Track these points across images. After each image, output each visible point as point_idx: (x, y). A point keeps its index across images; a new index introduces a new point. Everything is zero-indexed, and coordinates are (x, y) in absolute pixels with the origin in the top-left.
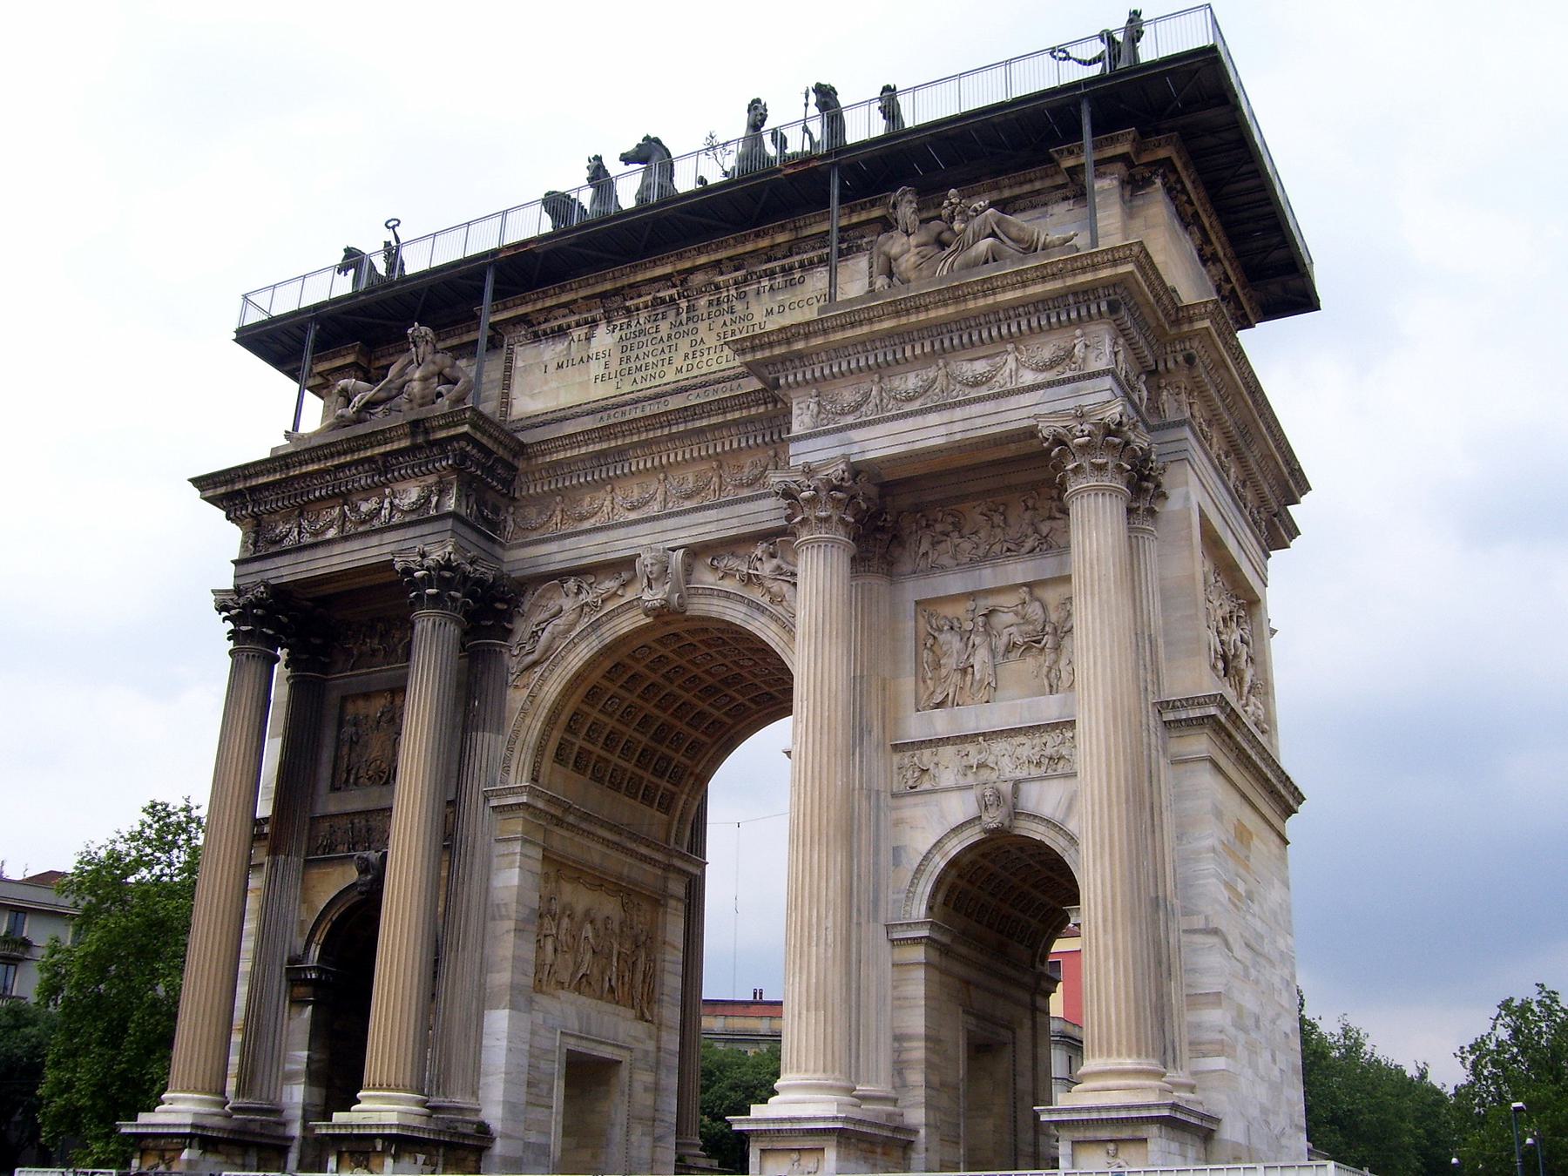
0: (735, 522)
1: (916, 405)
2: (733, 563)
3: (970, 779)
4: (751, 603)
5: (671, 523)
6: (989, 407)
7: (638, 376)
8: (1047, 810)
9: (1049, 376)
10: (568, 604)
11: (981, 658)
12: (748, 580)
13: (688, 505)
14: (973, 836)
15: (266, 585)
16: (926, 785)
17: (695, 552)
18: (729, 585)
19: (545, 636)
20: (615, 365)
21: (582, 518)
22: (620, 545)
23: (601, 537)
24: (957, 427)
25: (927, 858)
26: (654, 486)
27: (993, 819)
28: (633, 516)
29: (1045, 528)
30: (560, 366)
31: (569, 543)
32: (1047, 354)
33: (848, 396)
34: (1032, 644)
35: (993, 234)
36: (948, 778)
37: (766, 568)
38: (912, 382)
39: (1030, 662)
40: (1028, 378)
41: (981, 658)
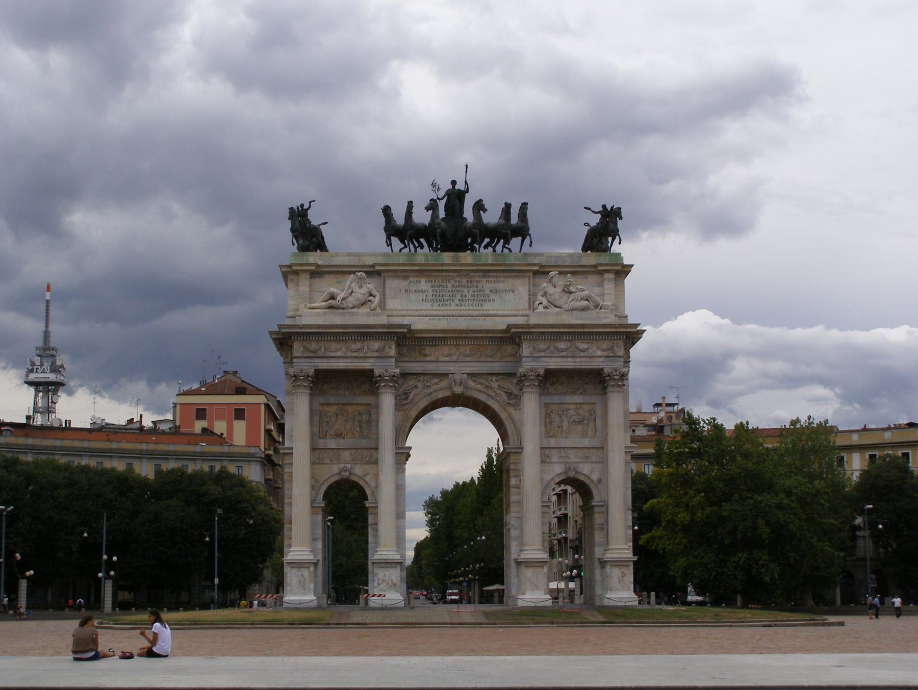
1: (564, 354)
2: (483, 381)
4: (489, 395)
6: (588, 360)
7: (440, 303)
8: (585, 472)
10: (420, 385)
11: (565, 424)
12: (487, 387)
13: (467, 359)
14: (563, 477)
16: (548, 460)
18: (479, 387)
19: (411, 396)
20: (430, 297)
21: (426, 356)
25: (549, 482)
26: (454, 350)
27: (572, 474)
28: (446, 359)
29: (586, 386)
30: (406, 291)
31: (421, 364)
32: (605, 346)
34: (580, 422)
36: (554, 459)
37: (495, 385)
38: (562, 345)
39: (579, 428)
40: (599, 353)
41: (565, 424)
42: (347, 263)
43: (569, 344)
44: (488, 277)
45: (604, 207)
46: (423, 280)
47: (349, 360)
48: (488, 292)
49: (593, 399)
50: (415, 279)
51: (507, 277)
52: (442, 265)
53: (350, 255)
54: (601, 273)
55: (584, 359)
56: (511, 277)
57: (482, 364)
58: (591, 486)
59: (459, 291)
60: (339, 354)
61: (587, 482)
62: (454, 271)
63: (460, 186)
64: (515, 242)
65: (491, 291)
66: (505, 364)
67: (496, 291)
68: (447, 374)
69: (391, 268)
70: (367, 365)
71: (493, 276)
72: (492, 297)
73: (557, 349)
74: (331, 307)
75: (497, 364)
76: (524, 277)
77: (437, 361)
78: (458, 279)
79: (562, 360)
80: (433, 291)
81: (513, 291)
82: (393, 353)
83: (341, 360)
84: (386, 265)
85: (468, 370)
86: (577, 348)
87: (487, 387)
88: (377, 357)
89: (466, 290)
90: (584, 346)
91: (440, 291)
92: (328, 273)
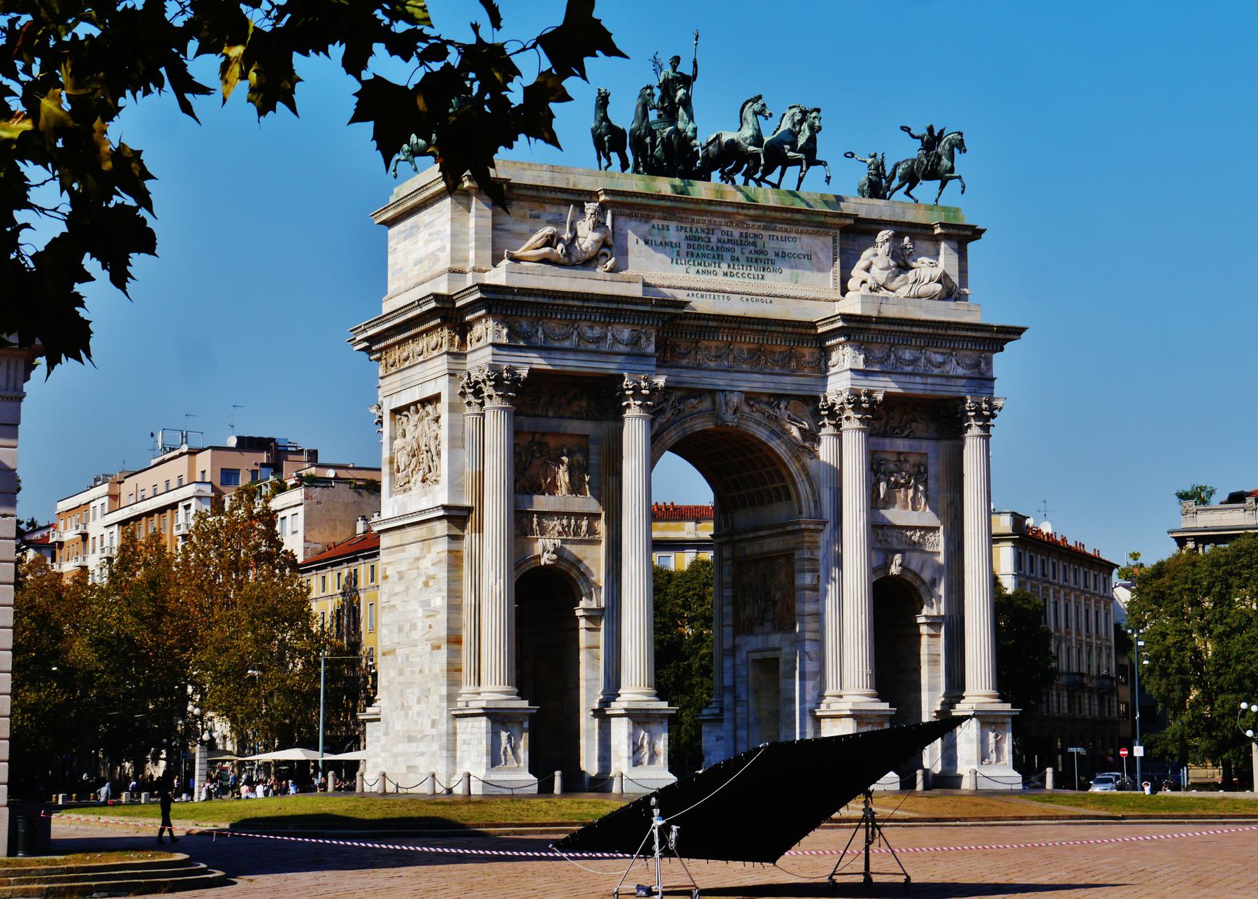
0: (772, 385)
1: (909, 369)
3: (878, 546)
4: (773, 432)
5: (737, 375)
6: (943, 381)
9: (968, 372)
13: (745, 367)
15: (531, 370)
17: (750, 397)
18: (756, 415)
22: (707, 381)
23: (695, 374)
24: (929, 387)
28: (712, 364)
29: (914, 425)
33: (878, 354)
35: (939, 282)
38: (907, 355)
40: (960, 371)
42: (547, 184)
43: (917, 354)
44: (774, 230)
45: (931, 129)
46: (673, 225)
47: (582, 357)
48: (771, 255)
49: (925, 446)
50: (661, 223)
51: (801, 233)
52: (697, 201)
53: (553, 169)
54: (936, 239)
55: (938, 381)
56: (807, 233)
57: (768, 378)
58: (922, 590)
59: (728, 250)
60: (567, 344)
61: (917, 583)
62: (724, 215)
63: (685, 68)
64: (793, 172)
65: (777, 255)
66: (802, 380)
67: (784, 255)
68: (712, 392)
69: (629, 200)
70: (610, 367)
71: (781, 230)
72: (778, 261)
73: (898, 359)
74: (544, 260)
75: (788, 380)
76: (827, 234)
77: (699, 367)
78: (725, 229)
79: (907, 379)
80: (689, 246)
81: (809, 258)
82: (651, 349)
83: (570, 356)
84: (623, 193)
85: (746, 387)
86: (929, 361)
87: (769, 417)
88: (628, 354)
89: (738, 249)
90: (939, 358)
91: (700, 247)
92: (520, 198)
